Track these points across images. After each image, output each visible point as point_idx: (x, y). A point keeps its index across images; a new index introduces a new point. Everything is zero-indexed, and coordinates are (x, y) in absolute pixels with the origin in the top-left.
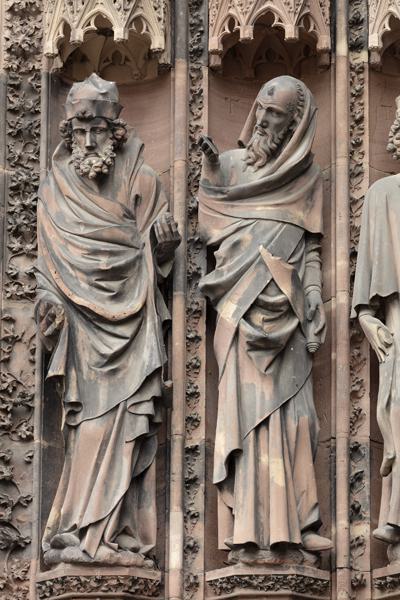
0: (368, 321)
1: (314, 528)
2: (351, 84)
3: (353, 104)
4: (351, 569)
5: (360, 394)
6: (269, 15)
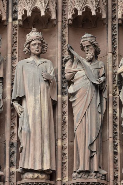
0: (16, 104)
2: (13, 31)
3: (13, 37)
4: (10, 181)
5: (14, 127)
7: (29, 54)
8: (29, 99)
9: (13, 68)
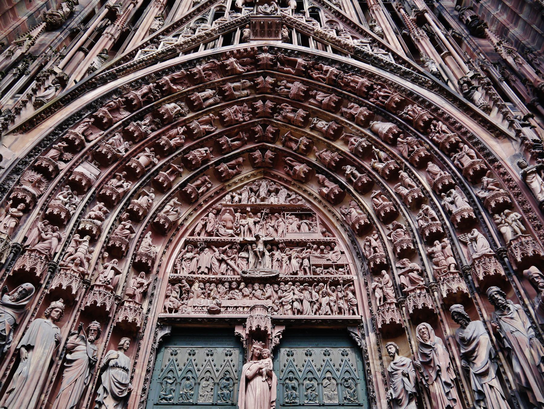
7: (48, 317)
8: (38, 350)
9: (29, 322)
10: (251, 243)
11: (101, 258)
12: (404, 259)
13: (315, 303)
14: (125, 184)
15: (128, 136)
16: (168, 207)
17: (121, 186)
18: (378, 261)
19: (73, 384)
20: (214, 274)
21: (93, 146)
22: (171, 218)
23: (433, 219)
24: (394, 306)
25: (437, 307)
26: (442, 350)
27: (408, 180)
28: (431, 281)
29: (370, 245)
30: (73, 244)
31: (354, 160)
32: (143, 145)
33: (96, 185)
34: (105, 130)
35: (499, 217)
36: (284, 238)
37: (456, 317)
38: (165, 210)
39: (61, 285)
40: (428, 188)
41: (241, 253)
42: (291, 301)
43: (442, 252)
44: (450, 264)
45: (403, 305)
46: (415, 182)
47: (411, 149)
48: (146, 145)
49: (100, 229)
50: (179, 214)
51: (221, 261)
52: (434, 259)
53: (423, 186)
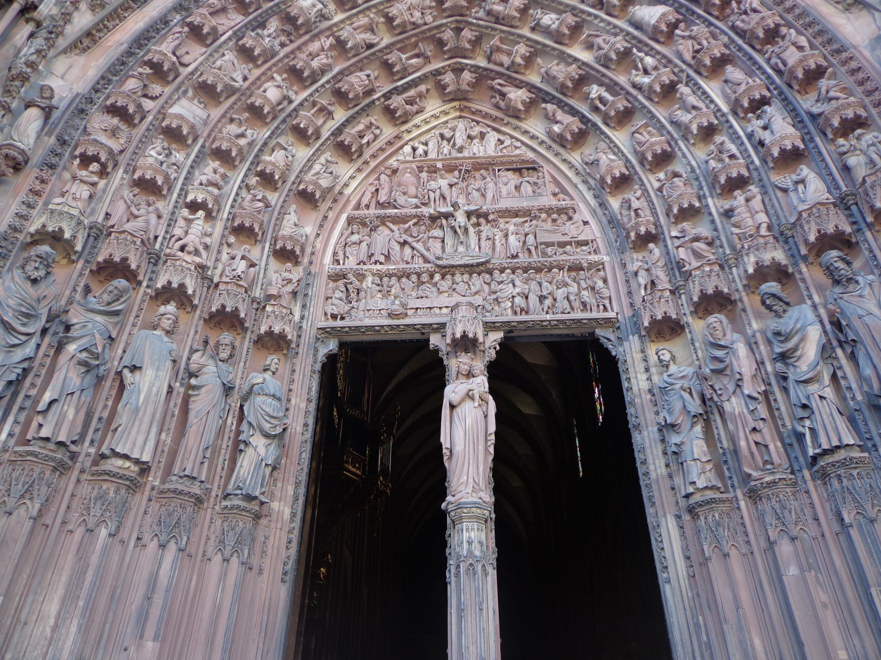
0: (126, 372)
1: (73, 442)
6: (126, 259)
8: (148, 372)
10: (447, 216)
11: (224, 242)
12: (684, 224)
13: (545, 298)
14: (249, 132)
15: (246, 54)
16: (317, 167)
17: (243, 135)
18: (643, 230)
19: (204, 419)
20: (394, 264)
21: (192, 73)
22: (325, 183)
23: (732, 157)
24: (668, 293)
25: (737, 290)
26: (744, 350)
27: (692, 100)
28: (728, 252)
29: (630, 207)
30: (181, 223)
31: (604, 75)
32: (269, 69)
33: (205, 135)
34: (208, 46)
35: (845, 143)
36: (497, 206)
37: (768, 302)
38: (313, 172)
39: (170, 283)
40: (725, 108)
41: (432, 232)
42: (510, 296)
43: (748, 206)
44: (760, 224)
45: (682, 291)
46: (703, 101)
47: (697, 47)
48: (274, 69)
49: (217, 200)
50: (337, 177)
51: (404, 244)
52: (733, 219)
53: (716, 105)
